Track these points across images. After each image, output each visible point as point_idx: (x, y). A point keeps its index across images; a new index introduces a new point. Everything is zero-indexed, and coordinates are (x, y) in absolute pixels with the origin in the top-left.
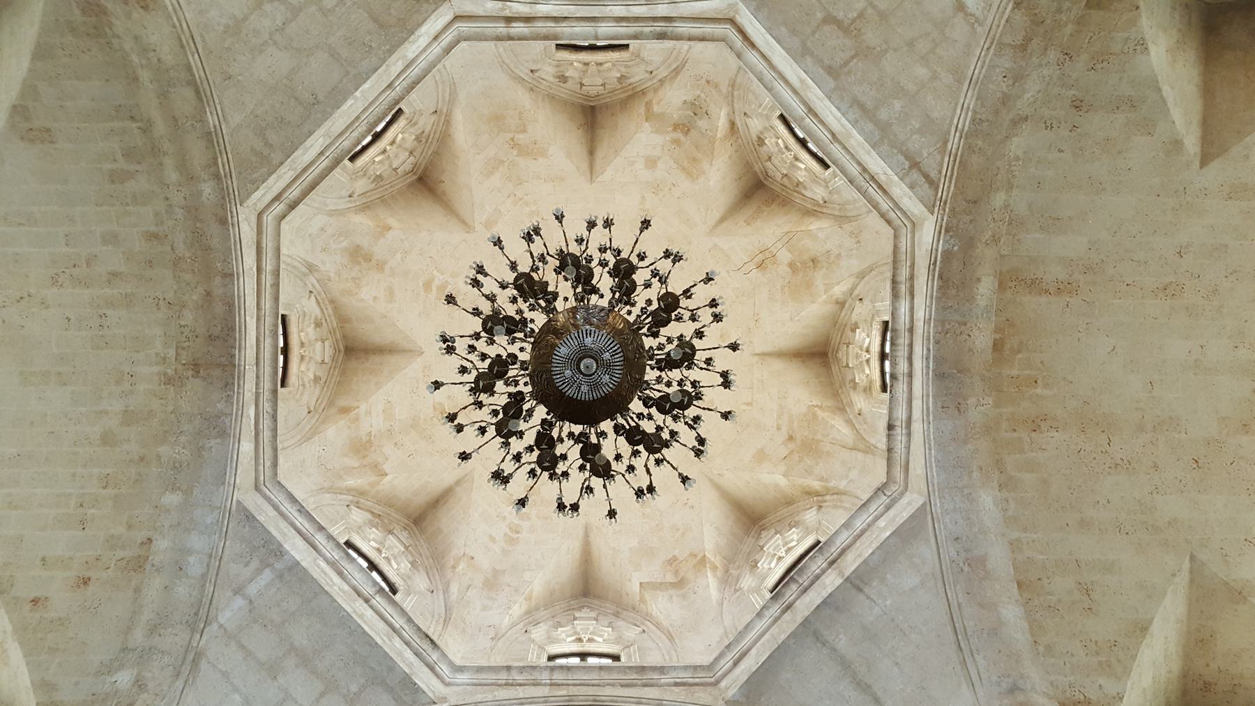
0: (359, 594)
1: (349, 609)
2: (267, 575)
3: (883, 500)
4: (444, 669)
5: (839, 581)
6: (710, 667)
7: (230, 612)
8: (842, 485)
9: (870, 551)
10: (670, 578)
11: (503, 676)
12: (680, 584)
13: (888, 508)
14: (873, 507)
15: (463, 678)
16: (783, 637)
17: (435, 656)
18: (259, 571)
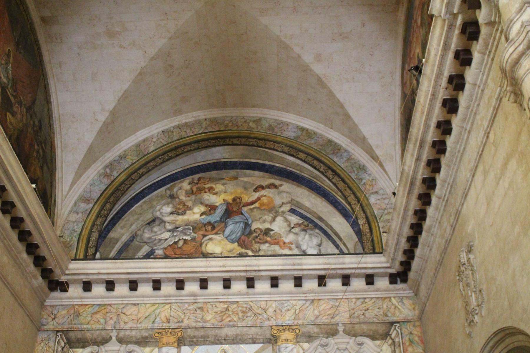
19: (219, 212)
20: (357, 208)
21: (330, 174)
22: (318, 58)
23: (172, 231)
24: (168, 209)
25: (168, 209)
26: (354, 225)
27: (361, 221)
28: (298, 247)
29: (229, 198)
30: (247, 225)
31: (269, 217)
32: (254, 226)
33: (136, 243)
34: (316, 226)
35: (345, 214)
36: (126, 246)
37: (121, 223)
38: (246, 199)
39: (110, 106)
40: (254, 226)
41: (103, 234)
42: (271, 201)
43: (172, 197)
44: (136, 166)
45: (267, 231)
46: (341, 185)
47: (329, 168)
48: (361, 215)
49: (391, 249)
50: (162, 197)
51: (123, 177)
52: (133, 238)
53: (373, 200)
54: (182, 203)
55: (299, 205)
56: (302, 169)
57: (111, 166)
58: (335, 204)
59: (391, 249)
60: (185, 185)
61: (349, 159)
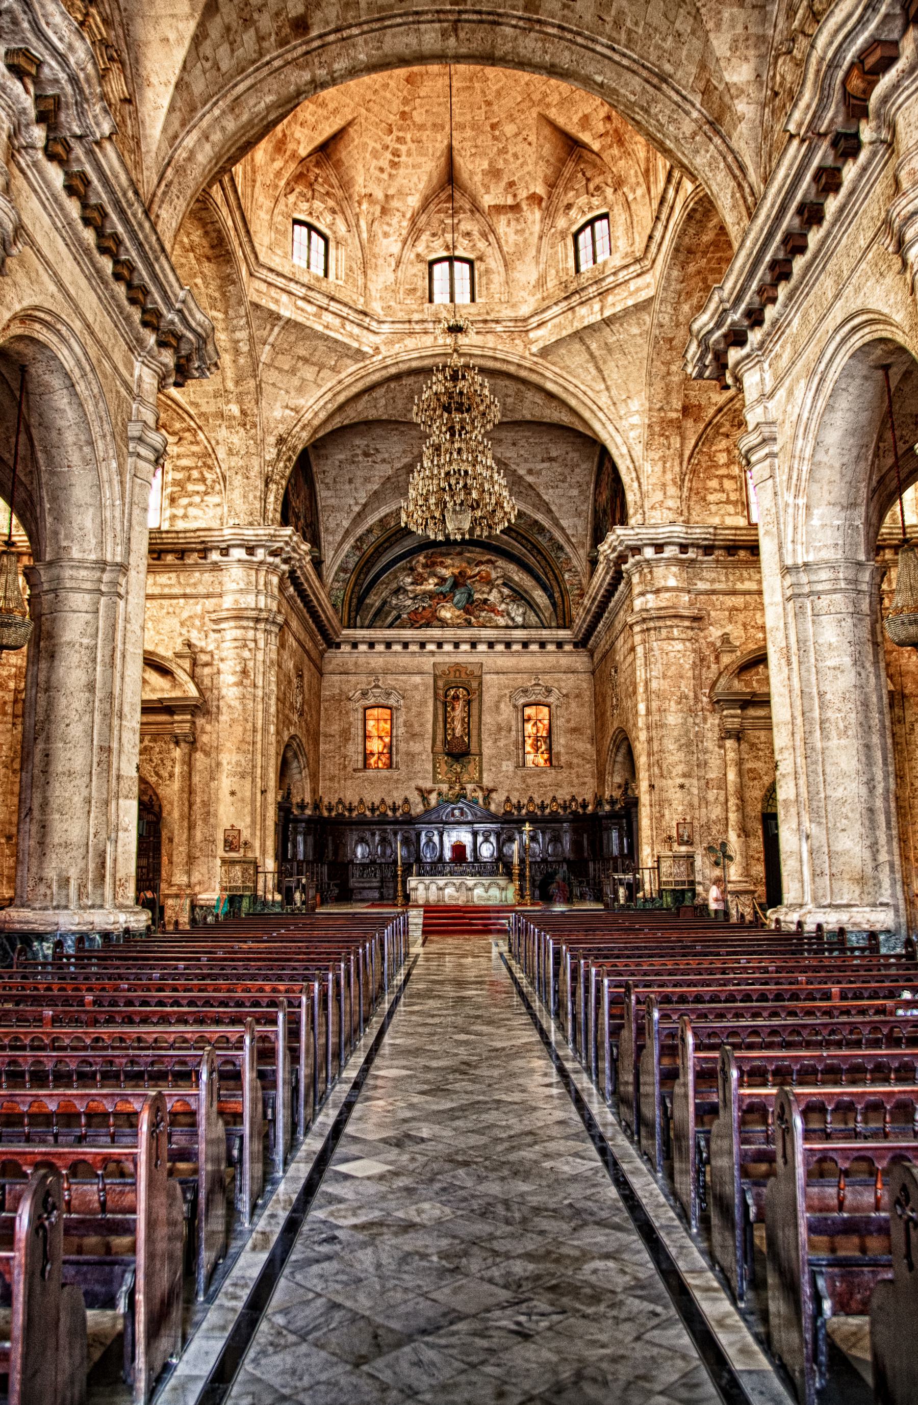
0: (321, 307)
1: (320, 328)
2: (276, 330)
3: (638, 266)
4: (374, 325)
5: (599, 318)
6: (525, 320)
7: (265, 354)
8: (631, 197)
9: (618, 308)
10: (510, 201)
11: (407, 326)
12: (515, 208)
13: (639, 275)
14: (632, 269)
15: (386, 328)
16: (565, 333)
17: (367, 320)
18: (272, 330)
19: (449, 583)
20: (554, 583)
21: (535, 552)
22: (530, 472)
23: (414, 598)
24: (409, 580)
25: (409, 580)
26: (551, 597)
27: (557, 595)
28: (509, 614)
29: (456, 571)
30: (470, 595)
31: (486, 589)
32: (477, 596)
33: (386, 608)
34: (523, 598)
35: (545, 588)
36: (379, 611)
37: (374, 591)
38: (470, 572)
39: (363, 501)
40: (477, 596)
41: (361, 599)
42: (488, 574)
43: (412, 569)
44: (381, 540)
45: (486, 600)
46: (543, 563)
47: (534, 546)
48: (556, 589)
49: (576, 628)
50: (404, 569)
51: (371, 550)
52: (385, 603)
53: (566, 576)
54: (420, 574)
55: (511, 579)
56: (513, 547)
57: (360, 539)
58: (537, 578)
59: (576, 628)
60: (422, 559)
61: (551, 539)
